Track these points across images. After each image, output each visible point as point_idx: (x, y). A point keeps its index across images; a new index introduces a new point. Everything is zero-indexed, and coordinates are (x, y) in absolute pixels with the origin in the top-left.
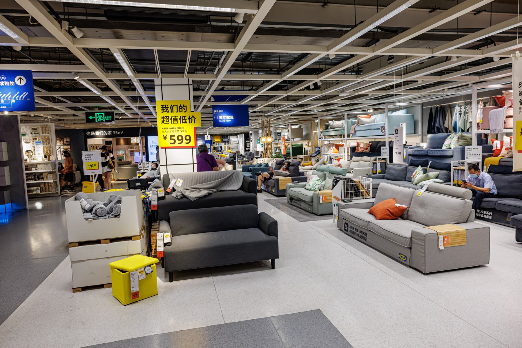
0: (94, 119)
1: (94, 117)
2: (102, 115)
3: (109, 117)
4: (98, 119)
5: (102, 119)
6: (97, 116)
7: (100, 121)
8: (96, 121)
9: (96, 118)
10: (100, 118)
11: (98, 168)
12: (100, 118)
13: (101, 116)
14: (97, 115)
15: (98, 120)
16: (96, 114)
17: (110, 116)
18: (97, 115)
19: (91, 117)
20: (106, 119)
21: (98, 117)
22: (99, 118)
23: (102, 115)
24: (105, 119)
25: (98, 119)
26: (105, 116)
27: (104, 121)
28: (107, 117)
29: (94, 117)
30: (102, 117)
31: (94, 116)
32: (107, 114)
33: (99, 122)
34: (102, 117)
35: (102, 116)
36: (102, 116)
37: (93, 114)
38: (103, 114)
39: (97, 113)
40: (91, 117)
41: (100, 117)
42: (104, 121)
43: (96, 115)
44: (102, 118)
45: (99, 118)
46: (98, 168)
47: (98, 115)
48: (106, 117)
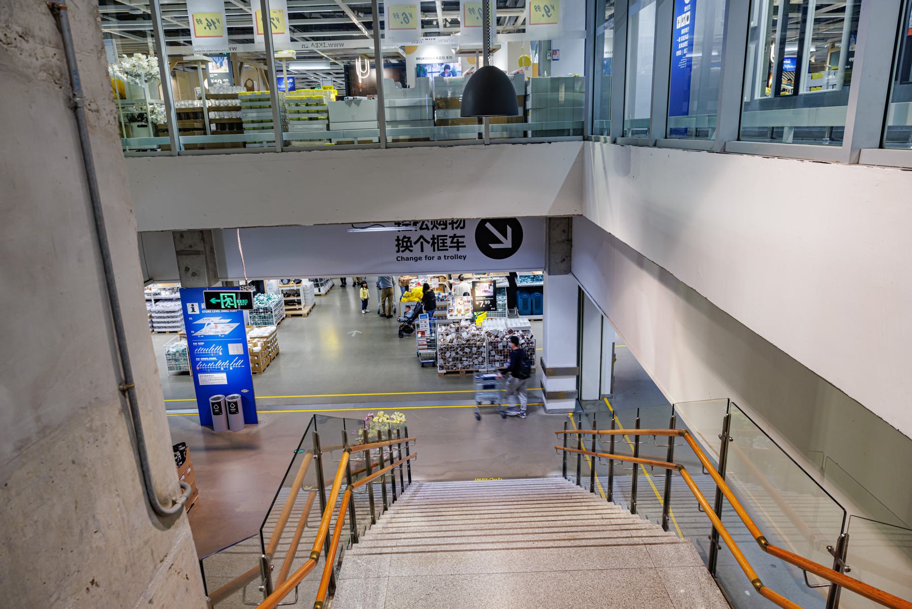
0: (220, 303)
1: (219, 301)
2: (232, 297)
4: (225, 303)
5: (232, 304)
7: (229, 307)
8: (223, 307)
9: (222, 301)
10: (229, 302)
12: (229, 302)
13: (230, 299)
14: (224, 296)
15: (226, 305)
16: (221, 295)
18: (224, 296)
19: (213, 301)
21: (225, 301)
23: (232, 297)
24: (237, 304)
25: (225, 303)
27: (236, 307)
29: (219, 301)
31: (218, 298)
35: (233, 299)
36: (233, 299)
37: (217, 296)
38: (234, 295)
39: (223, 294)
40: (213, 301)
41: (228, 300)
42: (236, 307)
43: (222, 297)
44: (233, 302)
47: (226, 297)
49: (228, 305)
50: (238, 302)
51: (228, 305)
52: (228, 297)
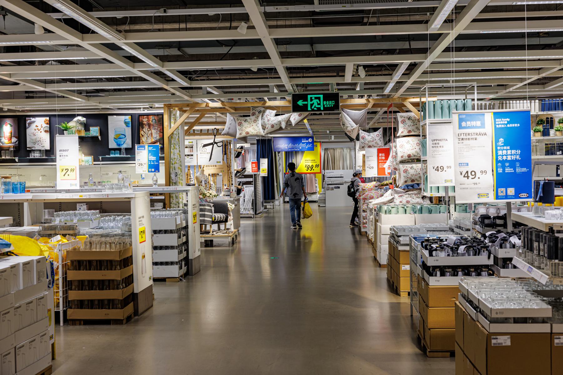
0: (307, 105)
1: (306, 103)
2: (319, 98)
3: (330, 102)
4: (312, 105)
5: (319, 106)
6: (311, 100)
7: (315, 109)
8: (309, 109)
9: (309, 103)
10: (316, 104)
11: (319, 172)
13: (318, 100)
14: (311, 98)
15: (313, 108)
16: (309, 96)
17: (332, 100)
19: (300, 103)
20: (326, 106)
21: (312, 103)
22: (313, 103)
23: (319, 98)
24: (324, 105)
25: (312, 105)
26: (324, 101)
27: (322, 109)
28: (328, 102)
29: (306, 103)
30: (319, 102)
31: (307, 101)
32: (327, 97)
33: (313, 110)
34: (319, 102)
35: (320, 101)
36: (320, 101)
37: (304, 98)
38: (321, 96)
39: (311, 96)
40: (300, 103)
41: (315, 101)
42: (322, 109)
44: (318, 104)
45: (313, 103)
46: (319, 172)
47: (313, 98)
48: (325, 102)
49: (315, 107)
50: (325, 103)
51: (315, 107)
52: (316, 98)
